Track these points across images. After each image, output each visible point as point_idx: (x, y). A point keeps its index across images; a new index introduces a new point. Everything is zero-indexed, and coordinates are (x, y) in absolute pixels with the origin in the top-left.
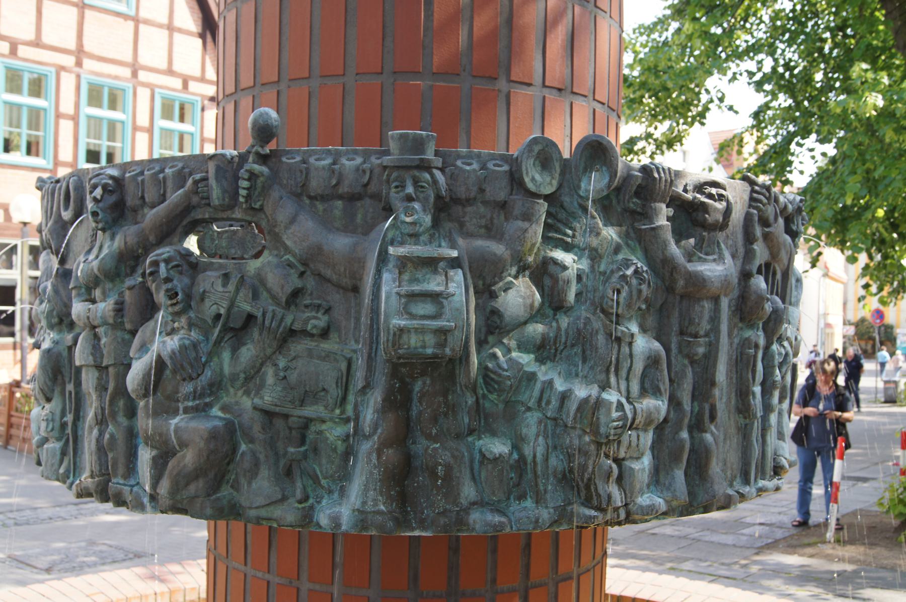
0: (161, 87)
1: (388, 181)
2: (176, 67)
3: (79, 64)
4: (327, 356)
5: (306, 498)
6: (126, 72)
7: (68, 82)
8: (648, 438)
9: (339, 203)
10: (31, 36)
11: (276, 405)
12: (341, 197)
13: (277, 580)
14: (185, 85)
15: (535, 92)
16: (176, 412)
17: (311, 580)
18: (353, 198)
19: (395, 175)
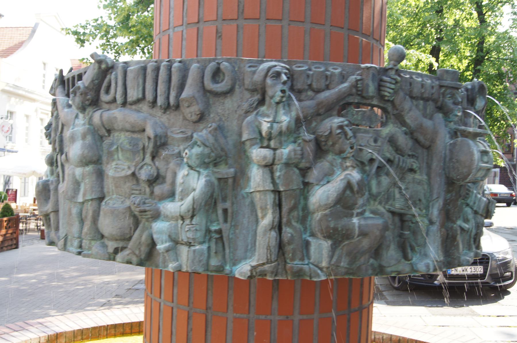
1: (443, 94)
4: (419, 182)
9: (421, 102)
11: (402, 209)
12: (423, 99)
13: (278, 318)
16: (352, 215)
17: (301, 313)
18: (426, 100)
19: (449, 91)
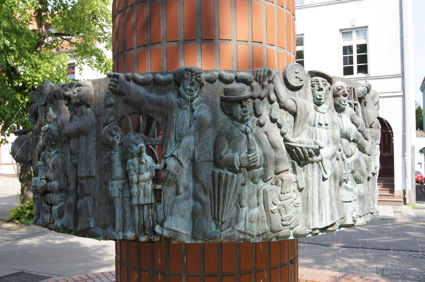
15: (134, 52)
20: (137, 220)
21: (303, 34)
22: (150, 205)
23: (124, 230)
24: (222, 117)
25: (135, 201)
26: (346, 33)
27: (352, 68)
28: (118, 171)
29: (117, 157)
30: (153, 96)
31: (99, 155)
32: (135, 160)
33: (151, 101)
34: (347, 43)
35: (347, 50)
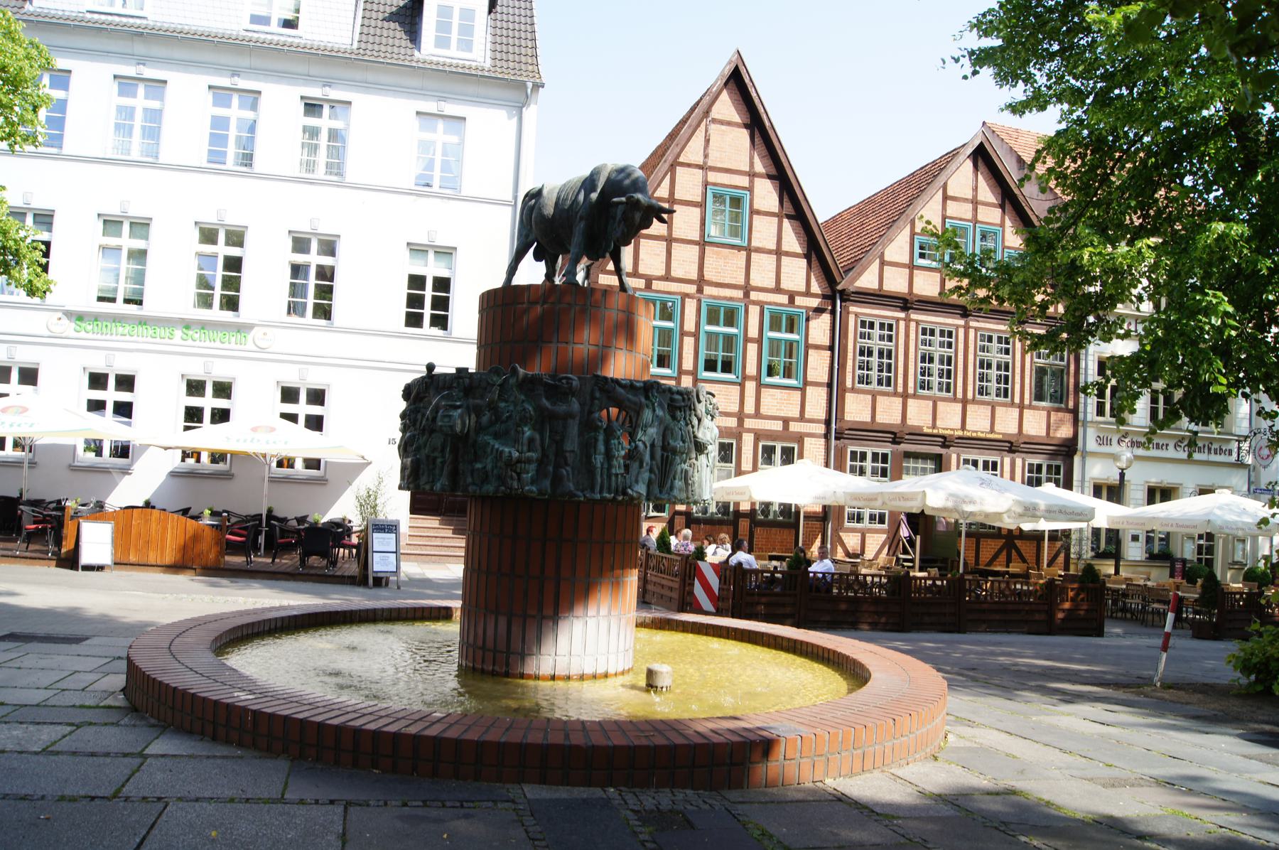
0: (770, 303)
2: (784, 285)
3: (700, 290)
5: (433, 481)
6: (739, 294)
7: (691, 306)
8: (533, 467)
10: (662, 272)
14: (792, 300)
20: (613, 484)
21: (339, 236)
22: (622, 474)
23: (601, 492)
24: (668, 417)
25: (614, 471)
26: (417, 250)
27: (421, 316)
28: (601, 447)
29: (601, 438)
30: (630, 396)
31: (581, 434)
32: (616, 441)
33: (629, 400)
34: (418, 271)
35: (416, 281)
